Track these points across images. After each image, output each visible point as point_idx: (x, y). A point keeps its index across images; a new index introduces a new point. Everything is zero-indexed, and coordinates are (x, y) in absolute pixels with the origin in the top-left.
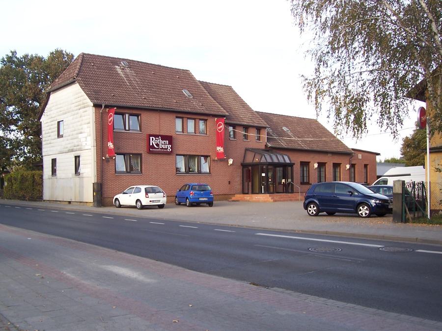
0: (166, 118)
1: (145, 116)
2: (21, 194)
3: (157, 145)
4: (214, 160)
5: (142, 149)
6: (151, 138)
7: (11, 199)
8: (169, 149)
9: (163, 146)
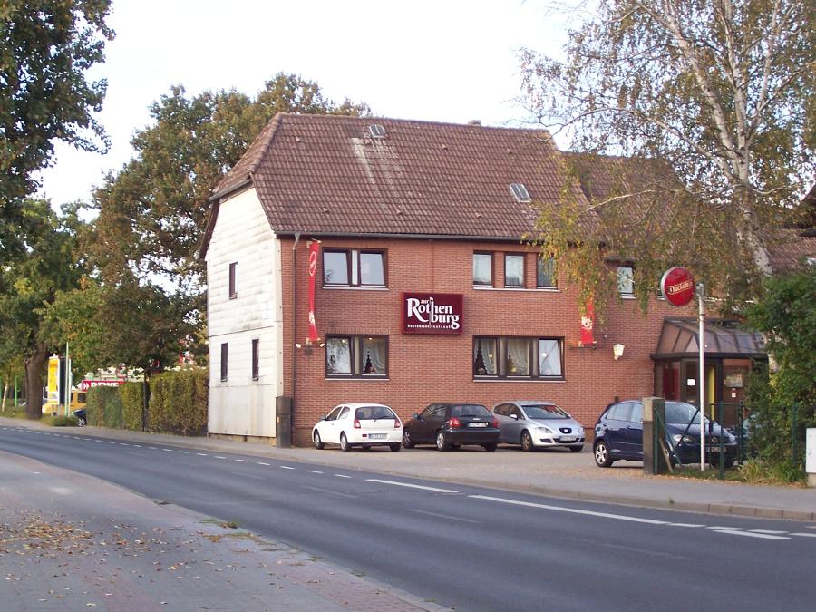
0: (446, 256)
1: (395, 253)
2: (176, 419)
3: (425, 316)
4: (573, 349)
5: (388, 324)
6: (410, 301)
7: (159, 431)
8: (455, 325)
9: (439, 318)
